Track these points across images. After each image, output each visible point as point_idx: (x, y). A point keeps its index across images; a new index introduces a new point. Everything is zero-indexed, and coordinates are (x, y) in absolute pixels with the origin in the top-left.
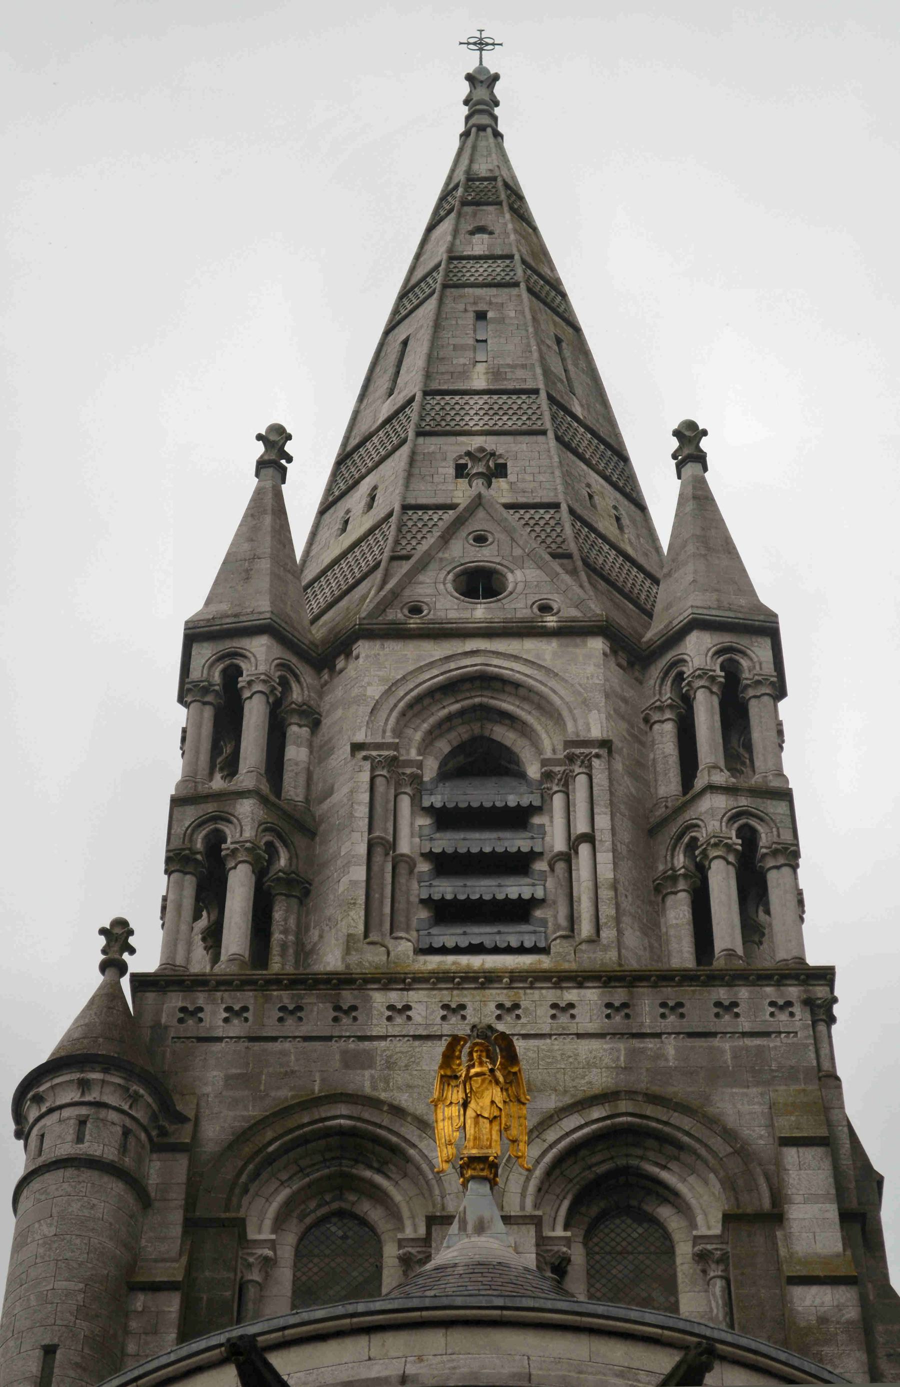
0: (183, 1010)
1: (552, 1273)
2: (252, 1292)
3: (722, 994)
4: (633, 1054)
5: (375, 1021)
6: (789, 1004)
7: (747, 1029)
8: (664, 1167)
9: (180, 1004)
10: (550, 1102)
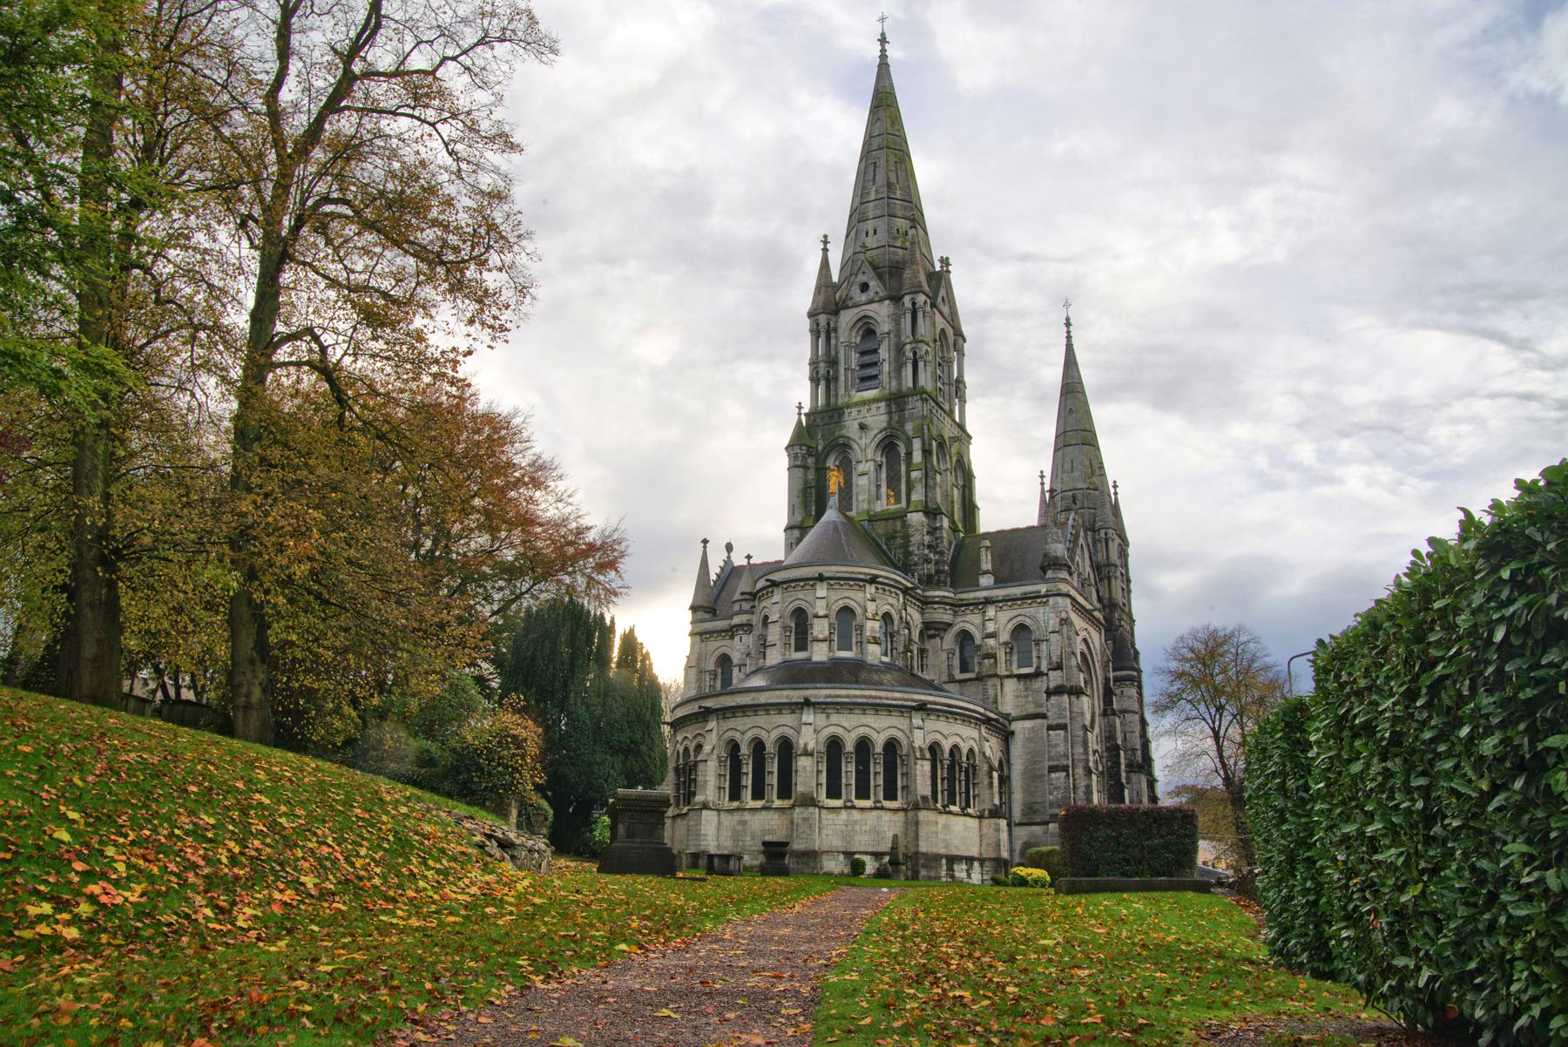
10: (875, 432)
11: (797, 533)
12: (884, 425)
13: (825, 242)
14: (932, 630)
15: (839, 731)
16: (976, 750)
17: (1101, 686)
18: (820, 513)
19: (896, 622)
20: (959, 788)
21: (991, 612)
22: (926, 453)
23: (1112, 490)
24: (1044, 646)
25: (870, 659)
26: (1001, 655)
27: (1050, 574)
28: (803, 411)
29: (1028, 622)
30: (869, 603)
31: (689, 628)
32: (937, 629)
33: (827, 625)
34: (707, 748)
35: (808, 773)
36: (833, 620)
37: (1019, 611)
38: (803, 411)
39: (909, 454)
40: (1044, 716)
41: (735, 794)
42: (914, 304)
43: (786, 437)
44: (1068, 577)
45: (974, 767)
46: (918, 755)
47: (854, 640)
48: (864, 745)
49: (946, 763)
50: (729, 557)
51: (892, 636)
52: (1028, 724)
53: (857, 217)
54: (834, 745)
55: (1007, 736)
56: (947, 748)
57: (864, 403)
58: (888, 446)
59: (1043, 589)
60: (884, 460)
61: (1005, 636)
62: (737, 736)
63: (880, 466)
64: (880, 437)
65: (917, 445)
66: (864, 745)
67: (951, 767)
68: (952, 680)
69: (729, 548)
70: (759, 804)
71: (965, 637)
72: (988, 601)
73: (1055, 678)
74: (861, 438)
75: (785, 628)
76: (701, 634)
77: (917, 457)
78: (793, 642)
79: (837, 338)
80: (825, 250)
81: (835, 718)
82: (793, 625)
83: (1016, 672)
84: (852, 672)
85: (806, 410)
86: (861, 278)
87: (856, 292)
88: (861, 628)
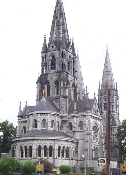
11: (38, 101)
12: (56, 78)
13: (45, 36)
14: (63, 122)
15: (40, 145)
16: (69, 147)
17: (100, 132)
19: (55, 121)
20: (65, 154)
21: (75, 118)
22: (64, 84)
23: (115, 85)
24: (85, 125)
25: (49, 130)
26: (76, 127)
27: (87, 111)
28: (40, 75)
29: (82, 121)
31: (17, 121)
32: (65, 122)
34: (17, 148)
35: (35, 152)
37: (81, 118)
39: (61, 85)
40: (84, 139)
41: (22, 157)
42: (62, 51)
43: (36, 80)
44: (90, 111)
45: (68, 150)
46: (56, 149)
48: (45, 147)
49: (62, 150)
50: (26, 105)
52: (82, 141)
53: (52, 30)
54: (40, 147)
55: (77, 143)
56: (62, 147)
58: (57, 82)
59: (85, 114)
61: (78, 123)
62: (22, 145)
63: (55, 87)
65: (62, 83)
66: (45, 147)
67: (63, 151)
68: (68, 132)
69: (26, 102)
70: (26, 158)
71: (71, 123)
72: (74, 116)
73: (86, 133)
75: (33, 123)
76: (20, 122)
77: (62, 85)
79: (47, 58)
80: (45, 37)
81: (39, 142)
82: (34, 123)
83: (80, 130)
84: (45, 133)
85: (41, 74)
86: (52, 45)
87: (51, 48)
88: (47, 124)
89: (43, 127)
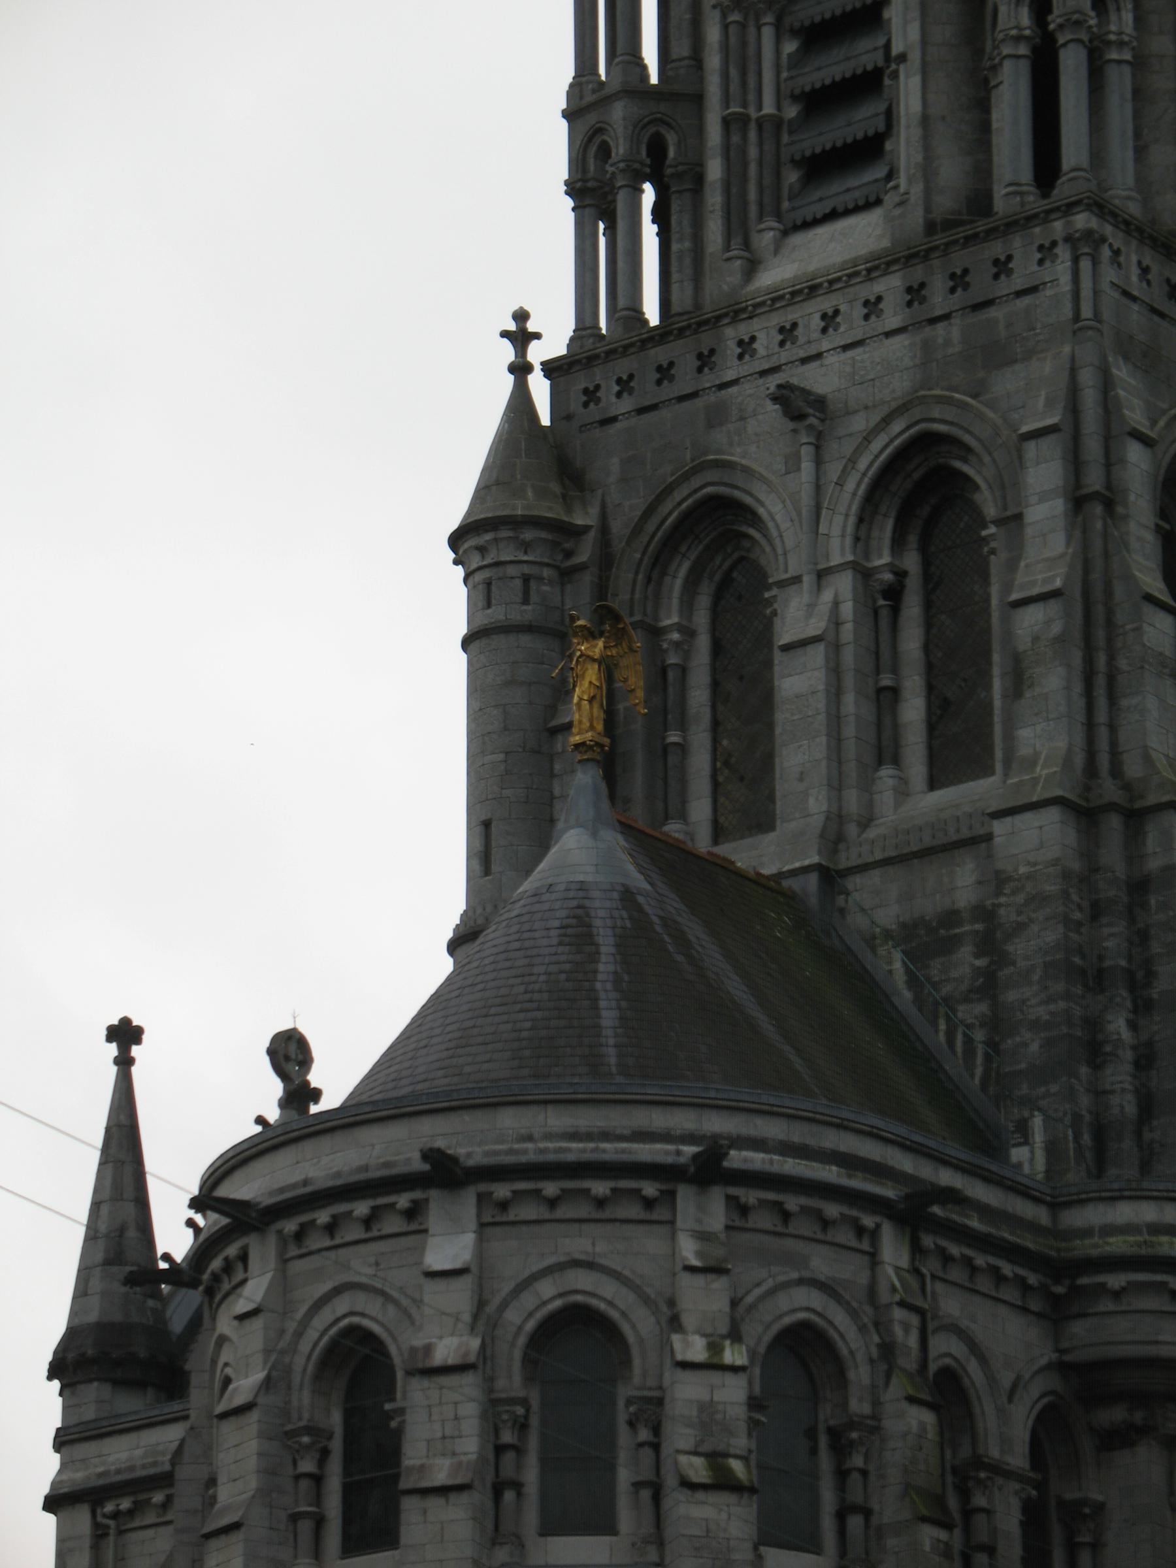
0: (586, 391)
1: (885, 599)
2: (671, 675)
3: (997, 249)
4: (927, 347)
5: (729, 364)
6: (1054, 244)
7: (1019, 288)
8: (965, 460)
9: (583, 386)
10: (859, 423)
12: (900, 385)
18: (543, 843)
19: (860, 1374)
30: (686, 1279)
33: (470, 1410)
36: (512, 1382)
38: (537, 353)
47: (624, 1477)
51: (840, 1445)
57: (810, 290)
60: (912, 562)
63: (894, 594)
64: (881, 448)
74: (793, 464)
78: (333, 1505)
82: (336, 1420)
89: (549, 1528)
